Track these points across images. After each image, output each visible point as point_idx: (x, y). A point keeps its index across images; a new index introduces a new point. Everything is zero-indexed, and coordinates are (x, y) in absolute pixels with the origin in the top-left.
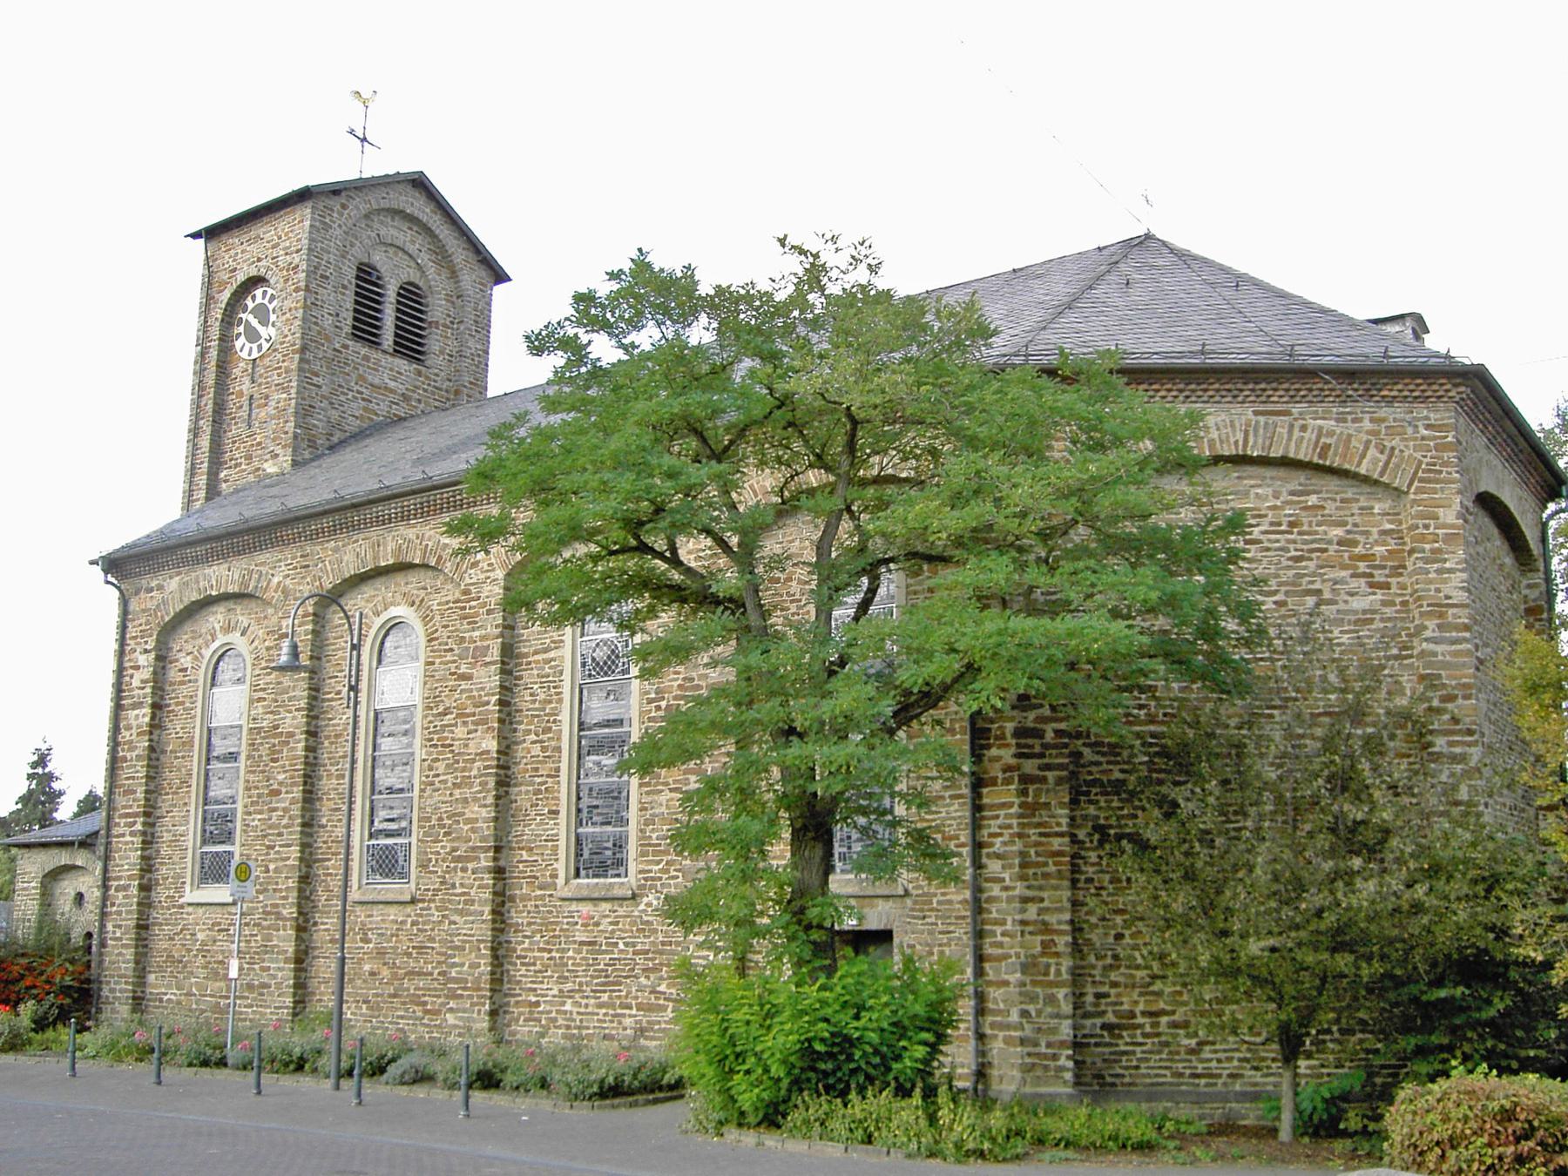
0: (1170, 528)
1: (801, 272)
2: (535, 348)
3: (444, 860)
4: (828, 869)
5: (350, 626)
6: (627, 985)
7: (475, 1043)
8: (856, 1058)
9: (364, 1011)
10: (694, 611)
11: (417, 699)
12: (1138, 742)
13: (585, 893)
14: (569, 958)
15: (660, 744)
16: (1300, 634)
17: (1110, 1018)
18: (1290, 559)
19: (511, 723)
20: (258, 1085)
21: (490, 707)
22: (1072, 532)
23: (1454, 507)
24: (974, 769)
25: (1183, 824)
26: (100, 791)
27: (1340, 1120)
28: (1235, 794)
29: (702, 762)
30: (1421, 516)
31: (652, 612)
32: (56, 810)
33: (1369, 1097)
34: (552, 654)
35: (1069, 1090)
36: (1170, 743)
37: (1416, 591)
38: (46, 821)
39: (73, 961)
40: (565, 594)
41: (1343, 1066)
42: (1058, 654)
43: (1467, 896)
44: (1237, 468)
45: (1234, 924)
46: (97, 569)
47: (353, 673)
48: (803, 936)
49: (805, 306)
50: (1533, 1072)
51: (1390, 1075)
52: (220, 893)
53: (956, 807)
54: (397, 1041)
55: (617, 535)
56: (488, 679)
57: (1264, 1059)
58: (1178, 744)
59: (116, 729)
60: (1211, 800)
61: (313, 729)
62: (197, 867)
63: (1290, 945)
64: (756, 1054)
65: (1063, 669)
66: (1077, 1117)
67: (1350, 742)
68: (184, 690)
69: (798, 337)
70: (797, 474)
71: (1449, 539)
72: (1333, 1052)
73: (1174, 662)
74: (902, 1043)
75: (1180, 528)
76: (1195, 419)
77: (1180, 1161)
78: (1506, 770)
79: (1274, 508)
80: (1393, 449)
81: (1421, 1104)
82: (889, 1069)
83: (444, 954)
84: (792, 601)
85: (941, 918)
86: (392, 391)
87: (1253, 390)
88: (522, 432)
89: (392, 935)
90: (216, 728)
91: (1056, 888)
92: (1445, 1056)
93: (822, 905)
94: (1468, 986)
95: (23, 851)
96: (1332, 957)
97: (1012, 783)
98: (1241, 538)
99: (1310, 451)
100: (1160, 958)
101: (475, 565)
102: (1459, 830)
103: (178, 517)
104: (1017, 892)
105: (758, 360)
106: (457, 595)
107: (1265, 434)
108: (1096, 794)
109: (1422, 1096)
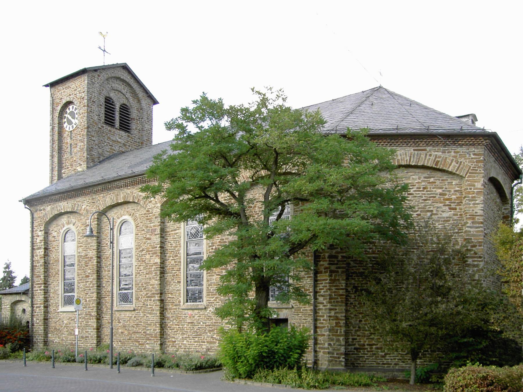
0: (383, 189)
1: (259, 101)
2: (168, 128)
3: (144, 297)
4: (268, 300)
5: (110, 222)
6: (203, 336)
7: (156, 353)
8: (276, 357)
9: (120, 344)
10: (224, 217)
11: (133, 246)
12: (369, 260)
13: (190, 307)
14: (185, 327)
15: (213, 260)
16: (424, 225)
17: (357, 346)
18: (423, 200)
19: (164, 254)
20: (86, 367)
21: (157, 249)
22: (349, 191)
23: (481, 182)
24: (315, 268)
25: (383, 286)
26: (29, 276)
27: (429, 378)
28: (400, 277)
29: (227, 266)
30: (469, 185)
31: (210, 218)
32: (14, 283)
33: (439, 371)
34: (177, 231)
35: (343, 368)
36: (379, 260)
37: (465, 211)
38: (11, 286)
39: (23, 330)
40: (181, 211)
41: (431, 362)
42: (343, 231)
43: (475, 310)
44: (407, 169)
45: (398, 317)
46: (22, 204)
47: (111, 238)
48: (259, 320)
49: (261, 113)
50: (494, 365)
51: (446, 365)
52: (71, 308)
53: (309, 280)
54: (131, 353)
55: (198, 192)
56: (156, 239)
57: (406, 359)
58: (382, 261)
59: (32, 256)
60: (392, 278)
61: (99, 256)
62: (63, 300)
63: (416, 324)
64: (244, 357)
65: (345, 236)
66: (346, 376)
67: (439, 260)
68: (55, 244)
69: (258, 124)
70: (258, 171)
71: (478, 193)
72: (428, 357)
73: (382, 234)
74: (291, 353)
75: (386, 189)
76: (393, 152)
77: (378, 390)
78: (492, 270)
79: (418, 183)
80: (461, 162)
81: (456, 374)
82: (286, 361)
83: (145, 326)
84: (256, 214)
85: (303, 315)
86: (120, 142)
87: (414, 142)
88: (165, 157)
89: (128, 321)
90: (66, 256)
91: (340, 306)
92: (465, 359)
93: (265, 311)
94: (474, 338)
95: (4, 296)
96: (430, 328)
97: (327, 273)
98: (406, 193)
99: (432, 163)
100: (374, 328)
101: (150, 202)
102: (474, 289)
103: (49, 186)
104: (328, 307)
105: (244, 132)
106: (145, 212)
107: (417, 157)
108: (354, 276)
109: (457, 371)
